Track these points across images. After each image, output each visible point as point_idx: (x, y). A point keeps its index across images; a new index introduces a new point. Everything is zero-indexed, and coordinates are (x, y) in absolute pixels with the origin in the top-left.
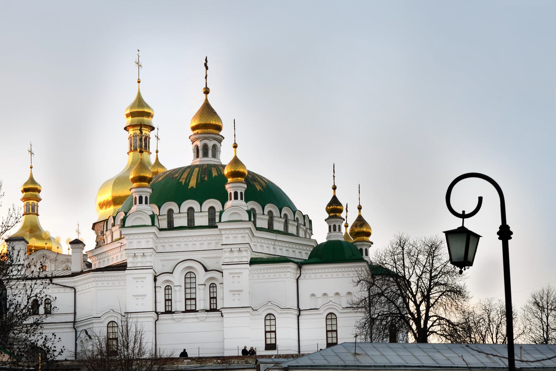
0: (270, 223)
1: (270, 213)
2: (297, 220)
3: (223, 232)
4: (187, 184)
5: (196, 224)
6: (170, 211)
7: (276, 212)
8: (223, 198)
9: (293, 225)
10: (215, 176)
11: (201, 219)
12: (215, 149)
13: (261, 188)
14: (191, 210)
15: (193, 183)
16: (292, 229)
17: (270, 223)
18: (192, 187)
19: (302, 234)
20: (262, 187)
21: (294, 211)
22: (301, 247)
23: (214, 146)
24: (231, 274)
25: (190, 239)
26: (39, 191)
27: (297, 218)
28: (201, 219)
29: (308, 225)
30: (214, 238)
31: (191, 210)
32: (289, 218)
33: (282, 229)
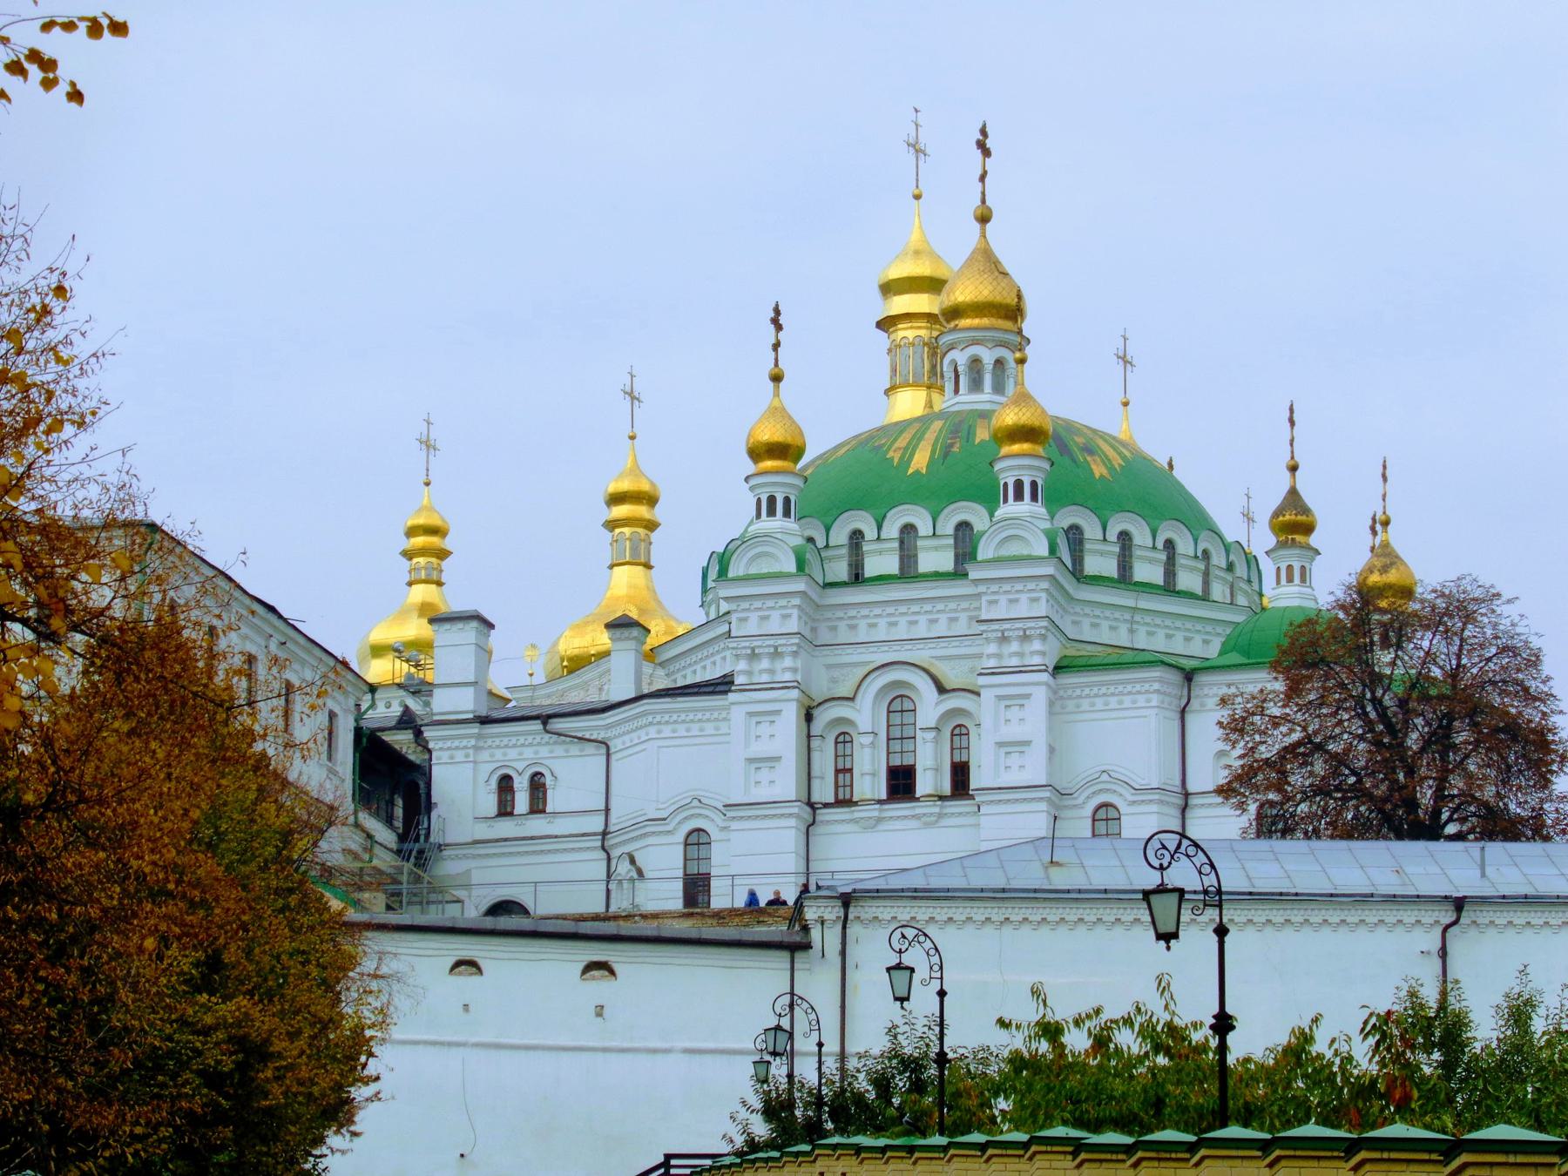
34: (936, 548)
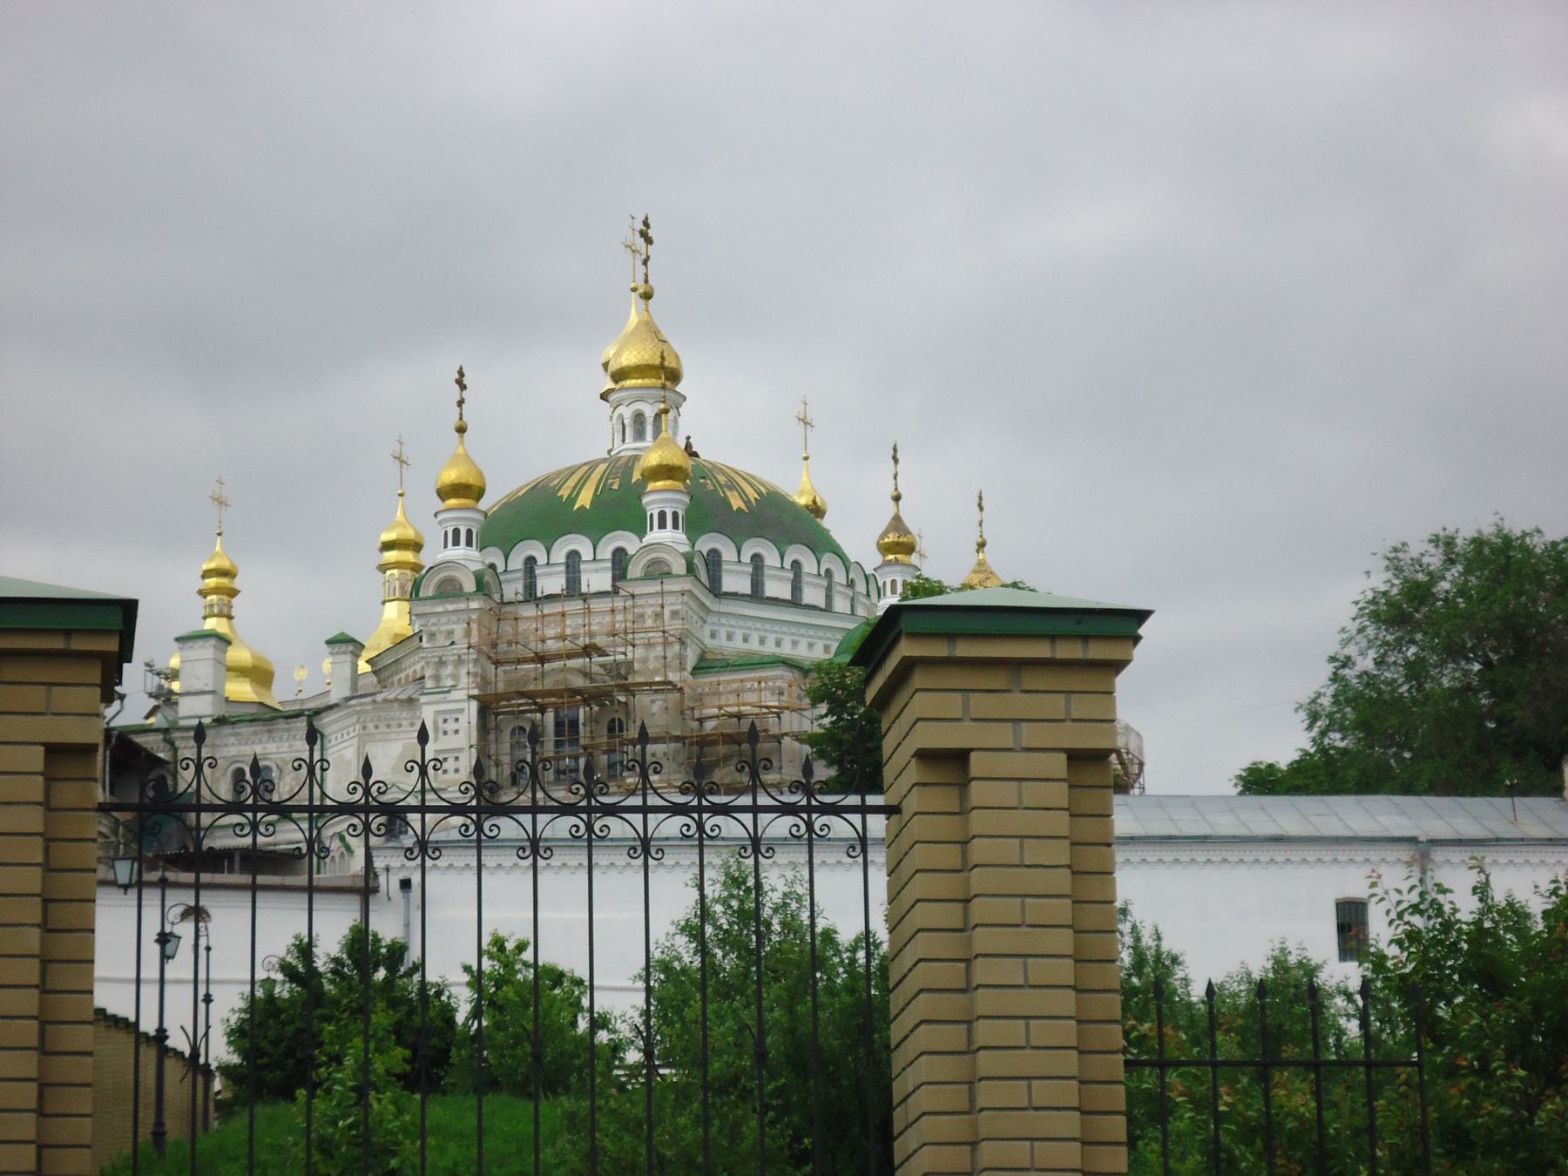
0: (757, 584)
4: (572, 500)
6: (531, 562)
7: (771, 558)
8: (639, 526)
11: (596, 579)
13: (742, 506)
15: (585, 499)
17: (757, 584)
27: (828, 571)
33: (786, 594)
34: (597, 571)
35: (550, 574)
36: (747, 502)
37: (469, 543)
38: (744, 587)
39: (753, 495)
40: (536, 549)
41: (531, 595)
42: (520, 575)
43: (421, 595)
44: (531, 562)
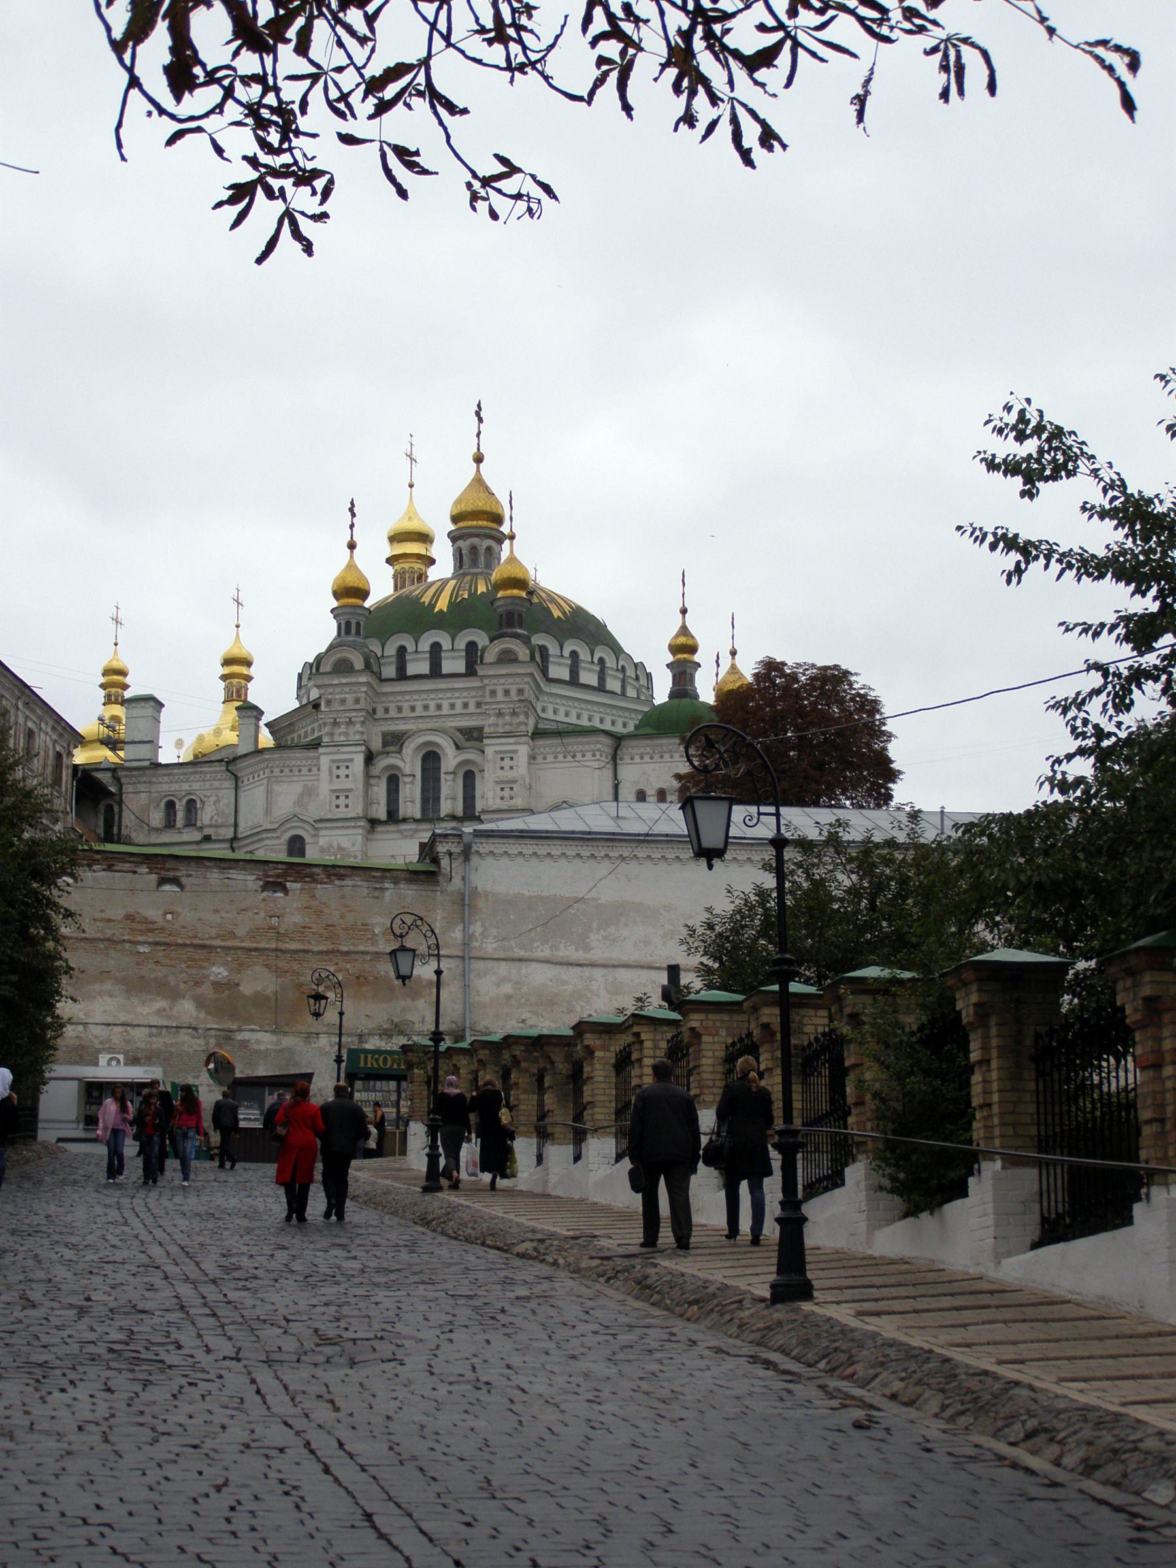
0: (574, 673)
1: (574, 654)
2: (623, 669)
3: (486, 681)
4: (432, 605)
5: (444, 671)
6: (402, 650)
7: (584, 655)
9: (615, 677)
10: (482, 593)
11: (453, 664)
12: (491, 554)
14: (436, 648)
15: (442, 604)
16: (613, 685)
17: (574, 673)
18: (441, 611)
19: (631, 692)
20: (564, 613)
21: (616, 649)
22: (627, 714)
23: (489, 549)
24: (498, 752)
25: (432, 696)
26: (249, 664)
27: (623, 667)
28: (453, 664)
29: (643, 681)
30: (473, 693)
31: (436, 648)
32: (608, 665)
33: (593, 680)
34: (454, 658)
35: (417, 660)
36: (564, 613)
37: (358, 633)
38: (565, 674)
39: (567, 608)
40: (408, 642)
41: (402, 675)
42: (393, 659)
43: (321, 670)
44: (402, 650)
